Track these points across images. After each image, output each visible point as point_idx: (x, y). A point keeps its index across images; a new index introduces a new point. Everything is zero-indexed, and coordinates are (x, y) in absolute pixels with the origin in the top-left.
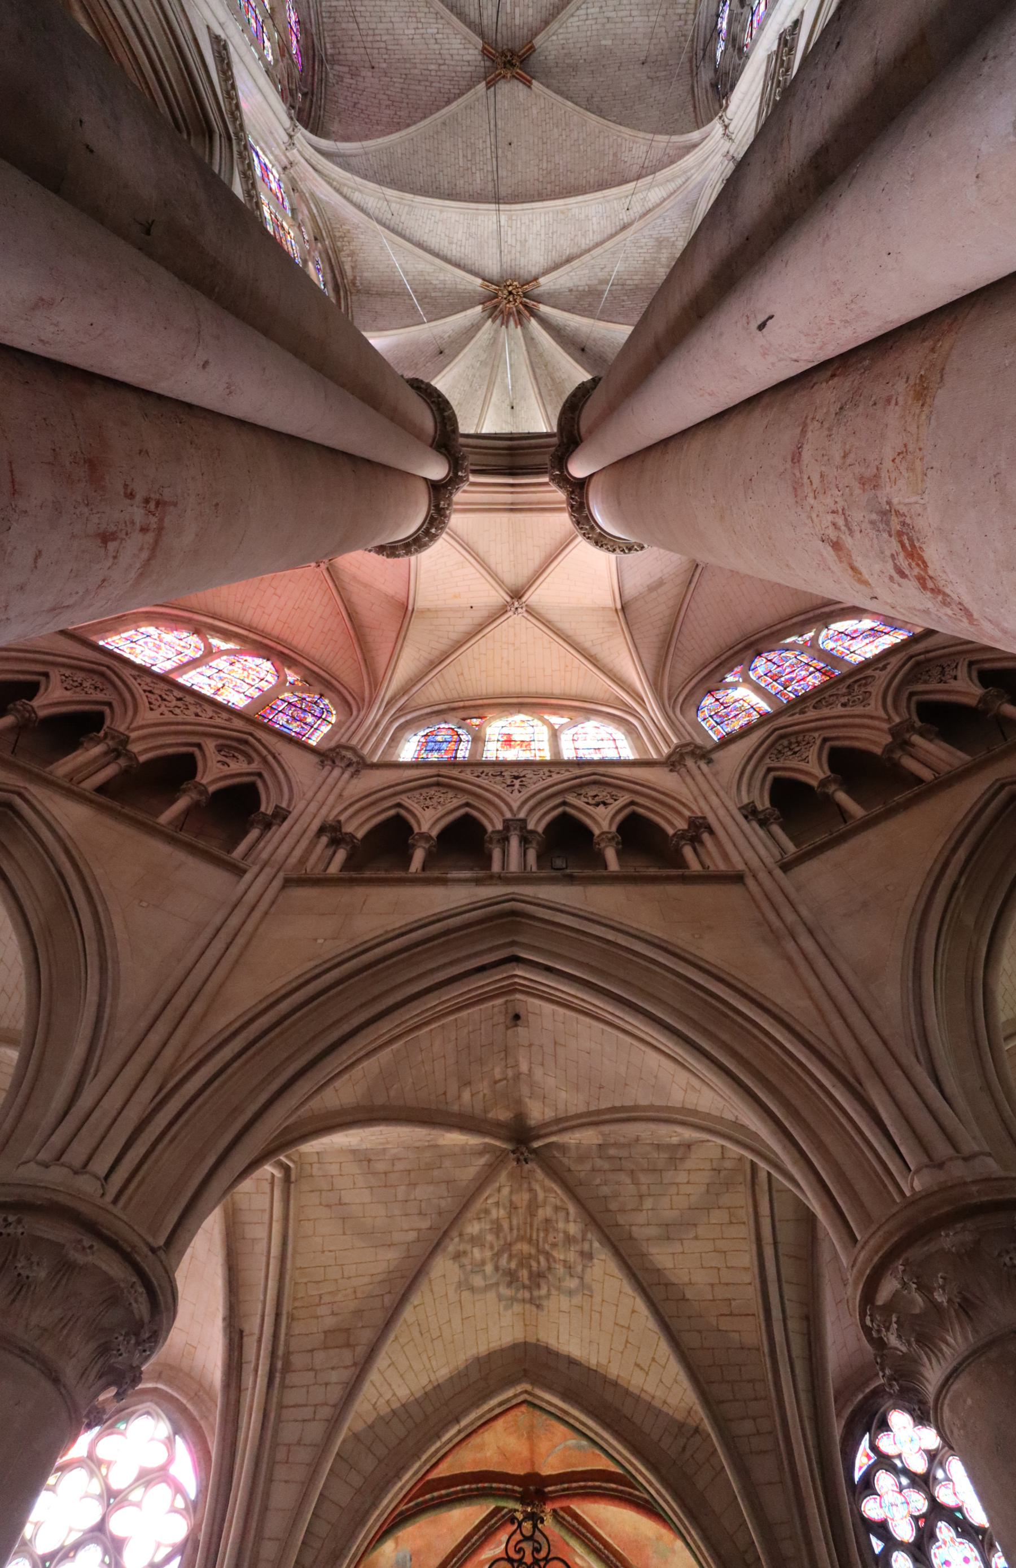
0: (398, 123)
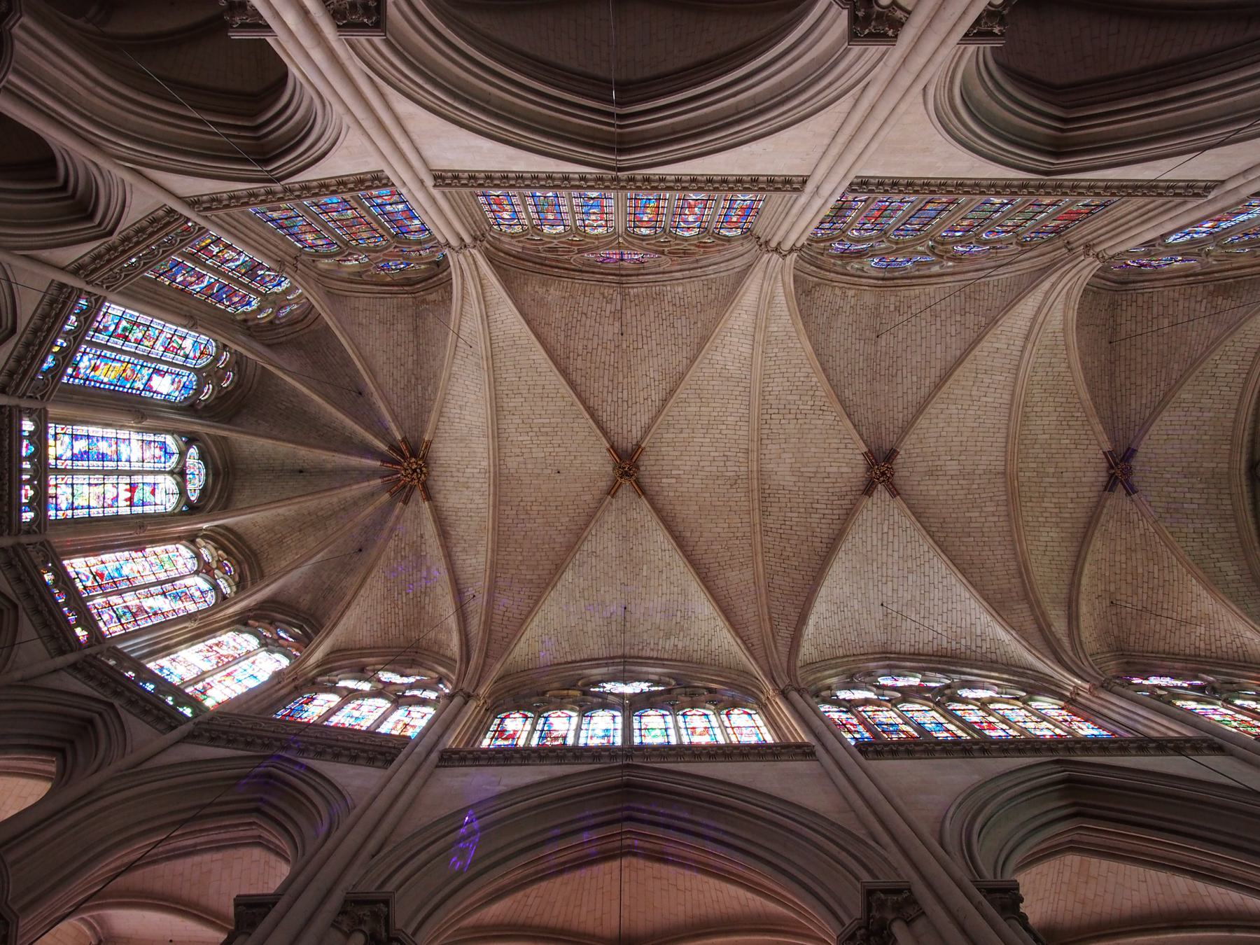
0: (568, 358)
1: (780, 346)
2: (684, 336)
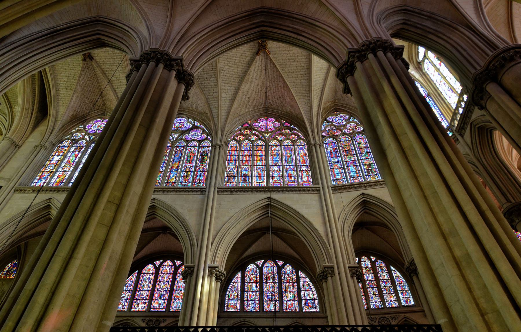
1: (213, 96)
2: (244, 95)
